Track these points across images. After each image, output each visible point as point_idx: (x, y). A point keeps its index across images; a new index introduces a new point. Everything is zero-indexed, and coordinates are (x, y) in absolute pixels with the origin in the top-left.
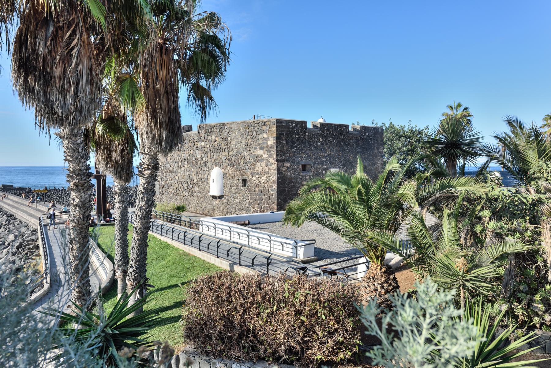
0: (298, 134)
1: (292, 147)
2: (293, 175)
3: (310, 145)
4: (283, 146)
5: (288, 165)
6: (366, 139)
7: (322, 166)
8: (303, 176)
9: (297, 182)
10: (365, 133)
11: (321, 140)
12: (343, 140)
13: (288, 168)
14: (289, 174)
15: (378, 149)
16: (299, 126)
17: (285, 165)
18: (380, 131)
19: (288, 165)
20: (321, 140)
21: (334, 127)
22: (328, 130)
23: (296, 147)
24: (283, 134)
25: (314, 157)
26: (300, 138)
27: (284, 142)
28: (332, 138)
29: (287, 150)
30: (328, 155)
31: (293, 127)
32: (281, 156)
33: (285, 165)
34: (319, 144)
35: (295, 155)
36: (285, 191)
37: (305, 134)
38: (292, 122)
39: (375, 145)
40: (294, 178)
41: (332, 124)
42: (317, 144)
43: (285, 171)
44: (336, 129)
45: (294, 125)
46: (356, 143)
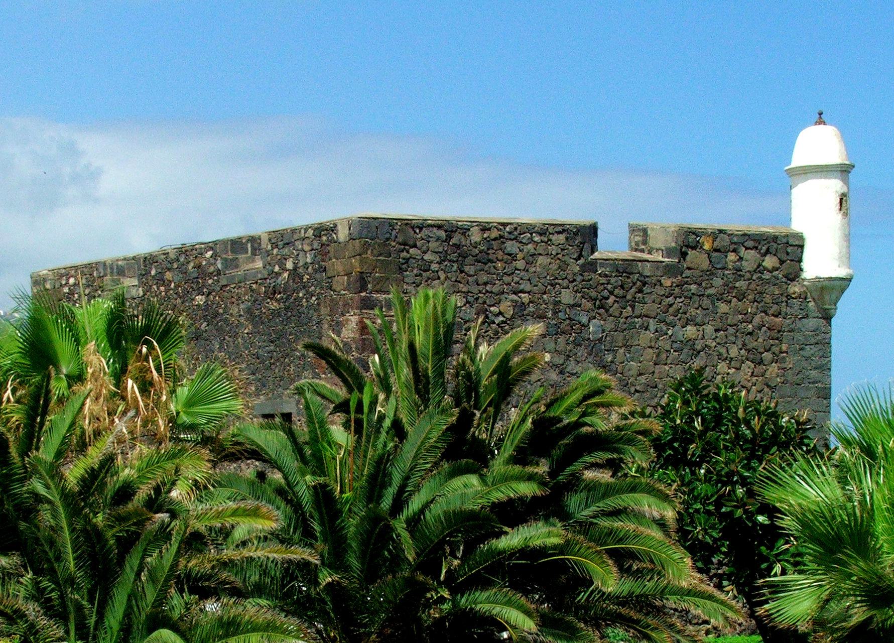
10: (282, 263)
39: (324, 311)
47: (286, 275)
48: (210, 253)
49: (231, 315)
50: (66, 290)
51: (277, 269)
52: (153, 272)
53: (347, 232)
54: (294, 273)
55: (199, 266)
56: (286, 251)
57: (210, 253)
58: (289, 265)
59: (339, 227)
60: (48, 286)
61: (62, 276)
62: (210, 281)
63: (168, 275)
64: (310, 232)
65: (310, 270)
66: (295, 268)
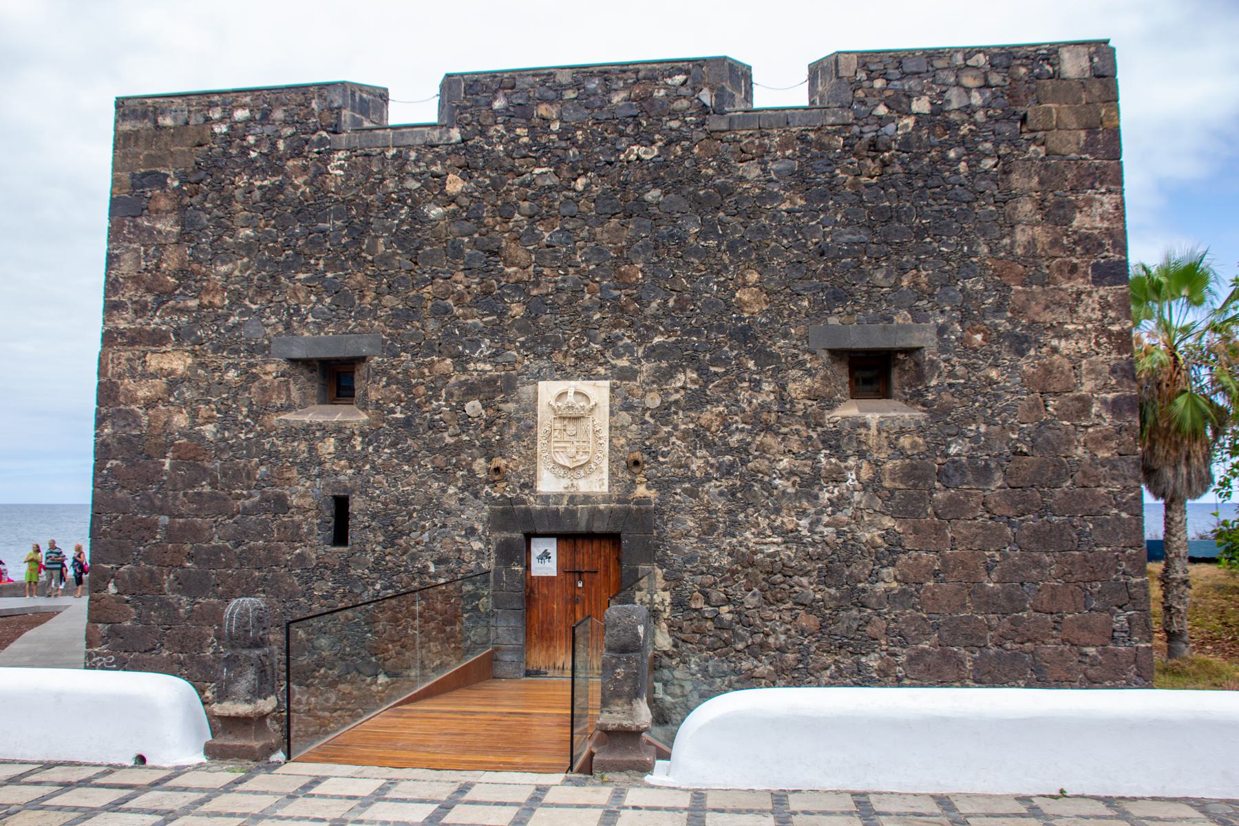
0: (273, 163)
1: (220, 253)
2: (209, 430)
3: (358, 233)
4: (161, 247)
5: (178, 363)
6: (906, 144)
7: (461, 361)
8: (291, 433)
9: (236, 475)
10: (900, 105)
11: (455, 185)
12: (657, 173)
13: (174, 382)
14: (181, 420)
15: (1056, 213)
16: (279, 114)
17: (154, 362)
18: (1072, 66)
19: (178, 363)
20: (455, 185)
21: (577, 85)
22: (520, 112)
23: (248, 248)
24: (161, 181)
25: (388, 300)
26: (280, 188)
27: (167, 226)
28: (558, 164)
29: (183, 274)
30: (519, 287)
31: (237, 133)
32: (141, 309)
33: (154, 362)
34: (435, 212)
35: (237, 298)
36: (151, 528)
37: (325, 157)
38: (229, 99)
40: (221, 446)
41: (546, 76)
42: (417, 217)
43: (150, 404)
44: (585, 99)
45: (240, 114)
46: (800, 180)
47: (910, 121)
48: (679, 79)
49: (742, 179)
50: (221, 129)
51: (882, 110)
52: (498, 104)
53: (1085, 63)
54: (937, 118)
55: (645, 100)
56: (912, 83)
57: (679, 79)
58: (921, 105)
59: (1065, 55)
60: (168, 121)
61: (212, 105)
62: (675, 124)
63: (543, 110)
64: (981, 59)
65: (980, 116)
66: (937, 110)
